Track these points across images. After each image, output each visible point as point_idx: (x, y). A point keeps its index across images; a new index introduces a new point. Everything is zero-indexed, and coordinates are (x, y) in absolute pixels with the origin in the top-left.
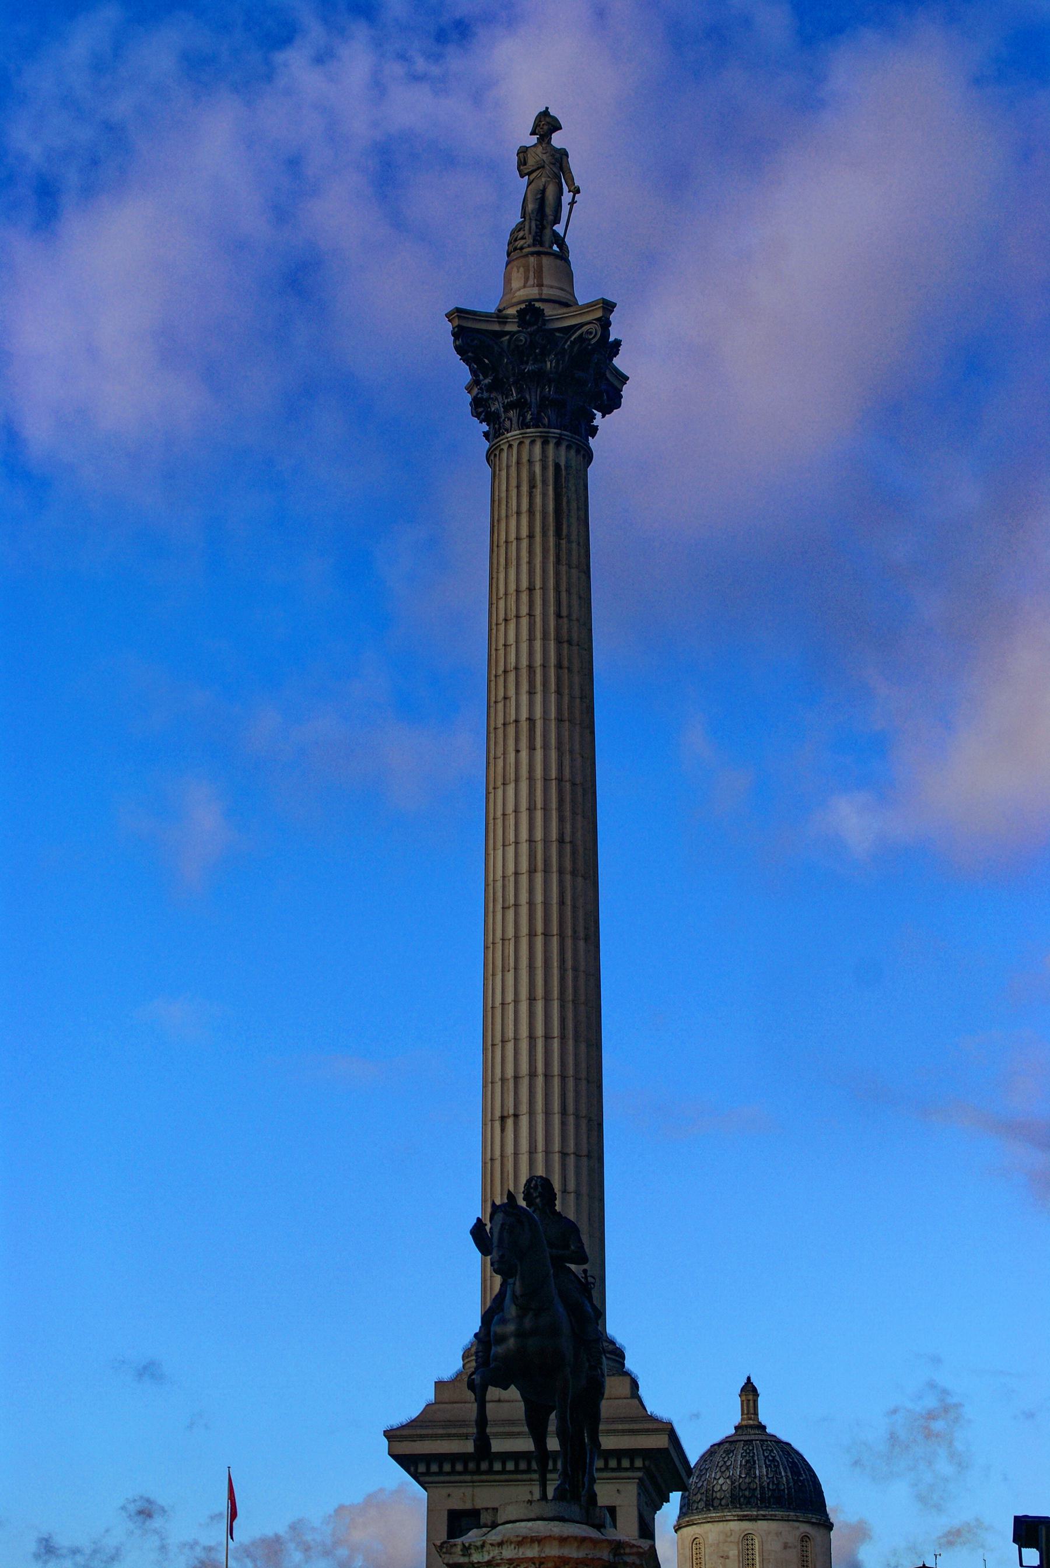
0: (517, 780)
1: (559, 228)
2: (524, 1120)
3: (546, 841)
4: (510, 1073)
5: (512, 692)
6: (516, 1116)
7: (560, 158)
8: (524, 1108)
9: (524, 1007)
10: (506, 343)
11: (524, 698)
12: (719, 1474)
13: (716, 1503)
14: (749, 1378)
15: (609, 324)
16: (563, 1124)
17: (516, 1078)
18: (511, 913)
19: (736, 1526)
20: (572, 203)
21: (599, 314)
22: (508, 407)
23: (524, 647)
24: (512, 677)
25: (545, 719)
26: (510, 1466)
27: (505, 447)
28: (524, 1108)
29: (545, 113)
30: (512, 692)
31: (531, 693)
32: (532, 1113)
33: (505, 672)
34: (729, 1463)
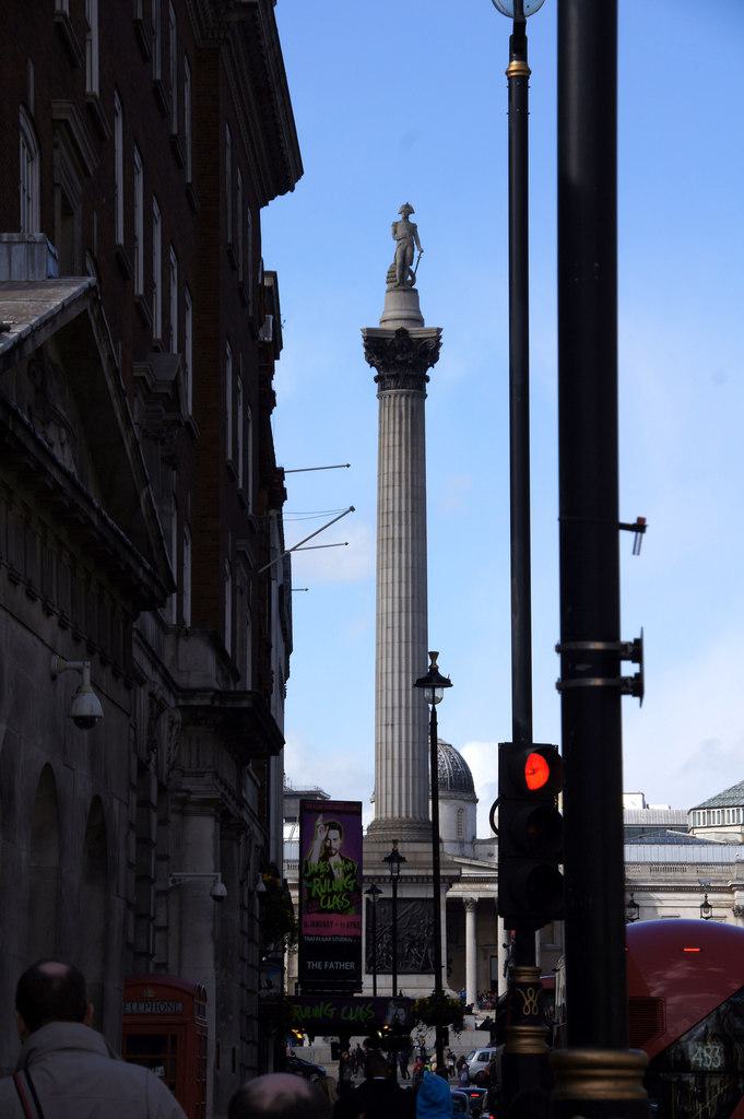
0: (393, 567)
1: (413, 268)
2: (396, 727)
3: (407, 597)
4: (390, 705)
6: (392, 725)
7: (412, 230)
8: (396, 722)
9: (396, 674)
11: (397, 527)
17: (393, 708)
23: (397, 501)
25: (407, 538)
28: (396, 722)
29: (407, 206)
30: (391, 523)
31: (400, 525)
32: (400, 724)
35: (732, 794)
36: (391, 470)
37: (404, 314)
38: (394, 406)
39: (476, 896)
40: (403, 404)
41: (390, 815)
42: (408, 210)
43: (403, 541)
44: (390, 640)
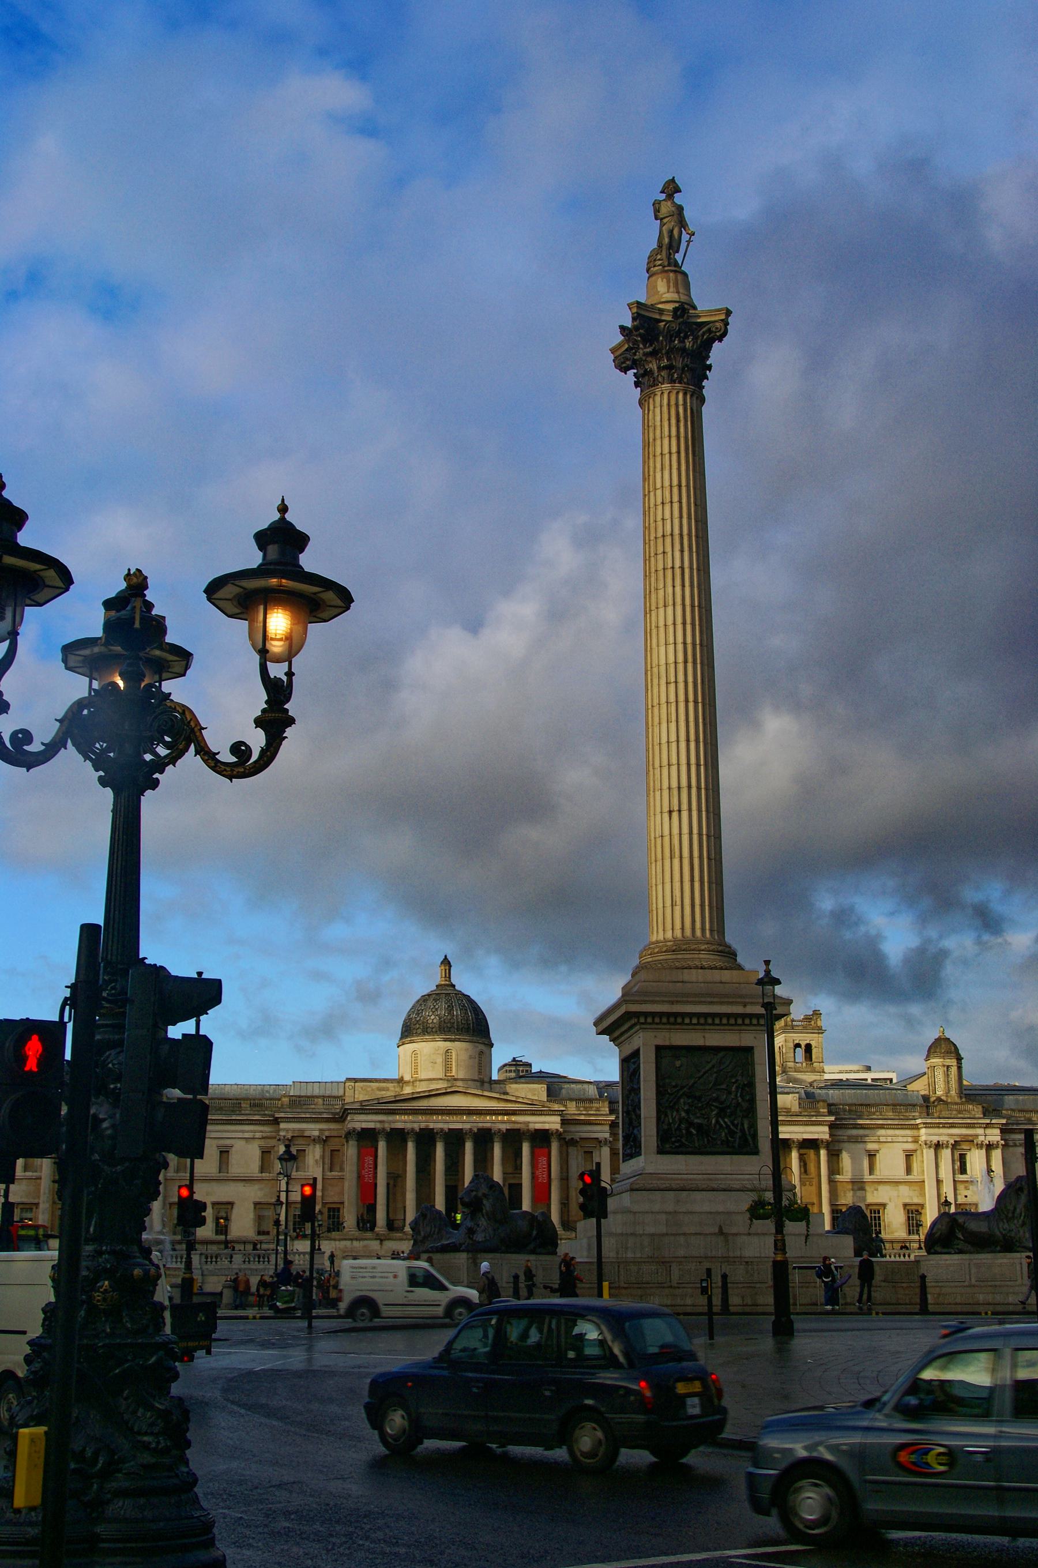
0: (674, 605)
1: (678, 257)
2: (685, 814)
4: (674, 784)
5: (669, 549)
6: (680, 811)
8: (685, 806)
10: (662, 326)
11: (677, 554)
12: (431, 1013)
13: (429, 1030)
14: (446, 956)
15: (728, 324)
16: (708, 818)
17: (679, 788)
18: (672, 687)
19: (444, 1045)
20: (689, 242)
21: (723, 317)
23: (676, 522)
24: (668, 540)
26: (664, 1020)
27: (659, 393)
28: (685, 806)
29: (673, 180)
30: (669, 549)
31: (682, 551)
32: (690, 810)
33: (663, 536)
34: (437, 1007)
36: (667, 483)
38: (669, 405)
39: (504, 1127)
40: (681, 401)
41: (678, 933)
42: (671, 188)
43: (687, 571)
44: (672, 698)
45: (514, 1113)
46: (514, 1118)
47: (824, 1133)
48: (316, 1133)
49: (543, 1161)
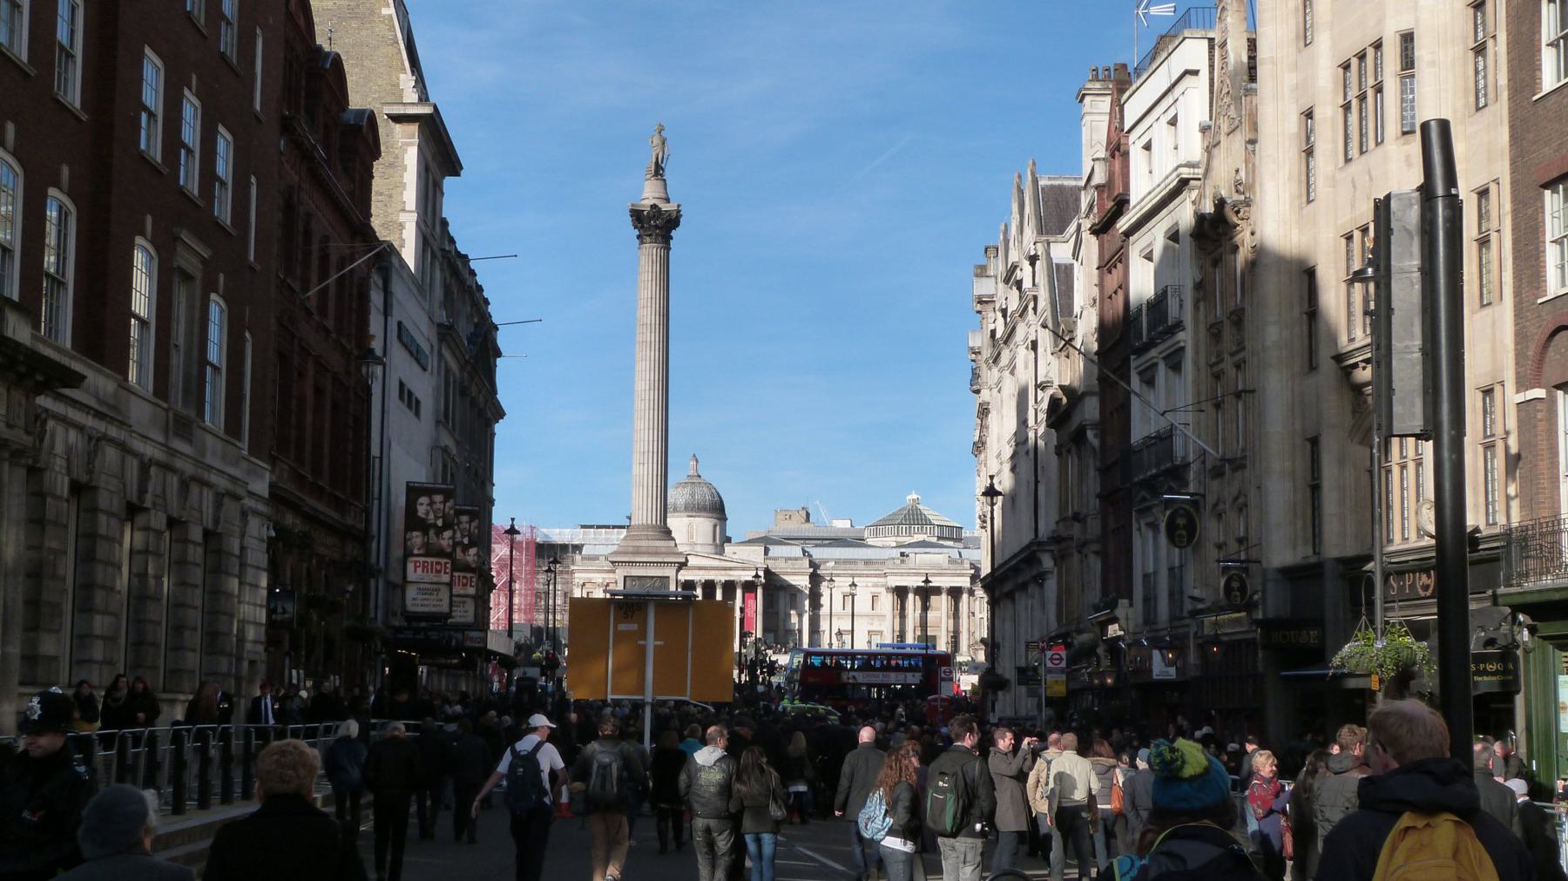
1: (663, 165)
2: (646, 465)
11: (649, 335)
17: (644, 452)
19: (686, 520)
22: (647, 235)
23: (649, 317)
28: (646, 462)
30: (645, 331)
31: (651, 333)
35: (891, 518)
37: (657, 195)
39: (723, 579)
41: (645, 522)
45: (730, 569)
46: (731, 572)
47: (966, 582)
48: (601, 581)
49: (750, 602)
